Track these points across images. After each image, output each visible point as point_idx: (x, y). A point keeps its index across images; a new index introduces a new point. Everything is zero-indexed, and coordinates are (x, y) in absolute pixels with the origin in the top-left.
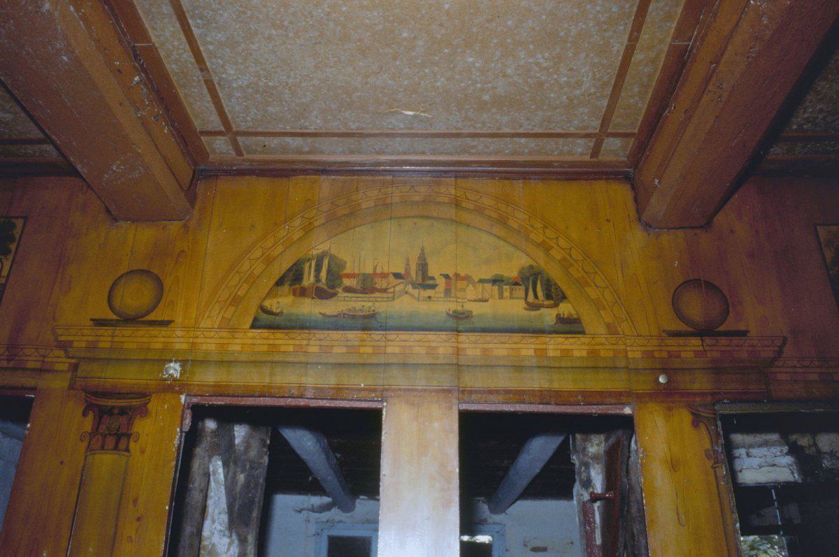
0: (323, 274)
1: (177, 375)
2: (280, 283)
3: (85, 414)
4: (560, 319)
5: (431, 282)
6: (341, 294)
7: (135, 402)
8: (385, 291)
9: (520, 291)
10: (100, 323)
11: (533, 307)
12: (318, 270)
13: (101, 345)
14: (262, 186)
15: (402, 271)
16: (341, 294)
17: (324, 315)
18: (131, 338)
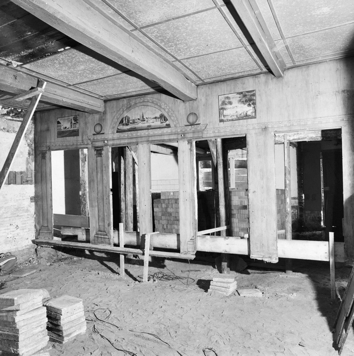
0: (127, 120)
1: (106, 143)
2: (120, 123)
3: (95, 151)
4: (166, 125)
5: (144, 120)
6: (130, 124)
7: (101, 148)
8: (137, 123)
9: (159, 119)
10: (94, 135)
11: (162, 123)
12: (126, 120)
13: (95, 139)
14: (114, 102)
15: (139, 118)
16: (130, 124)
18: (99, 137)
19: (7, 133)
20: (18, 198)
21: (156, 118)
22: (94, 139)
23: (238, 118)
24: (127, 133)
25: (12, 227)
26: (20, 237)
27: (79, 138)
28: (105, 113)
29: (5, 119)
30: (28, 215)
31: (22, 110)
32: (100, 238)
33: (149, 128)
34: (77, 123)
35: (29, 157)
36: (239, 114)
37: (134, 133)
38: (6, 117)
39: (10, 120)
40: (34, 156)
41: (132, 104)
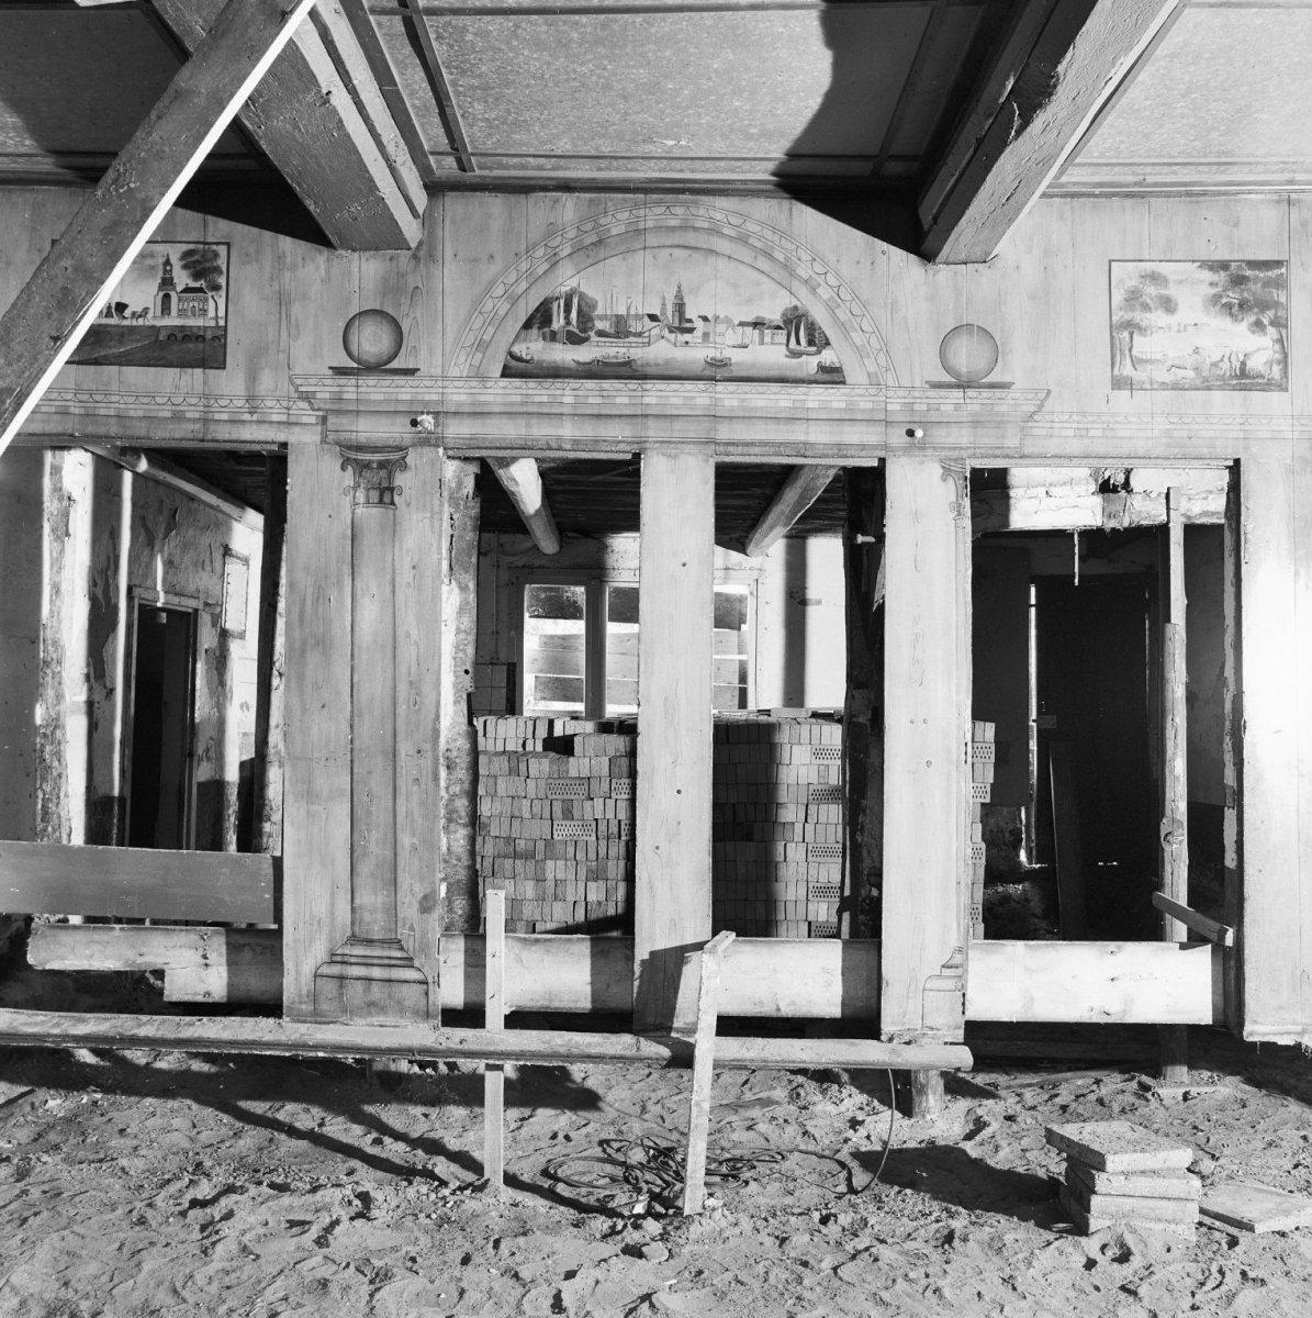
2: (527, 325)
4: (822, 368)
5: (688, 325)
7: (393, 456)
8: (640, 335)
10: (340, 371)
11: (795, 354)
12: (568, 310)
15: (658, 312)
17: (579, 363)
18: (375, 389)
21: (757, 324)
23: (1206, 380)
24: (575, 384)
27: (229, 383)
28: (425, 254)
32: (359, 986)
33: (716, 372)
36: (1208, 362)
37: (621, 394)
41: (614, 232)
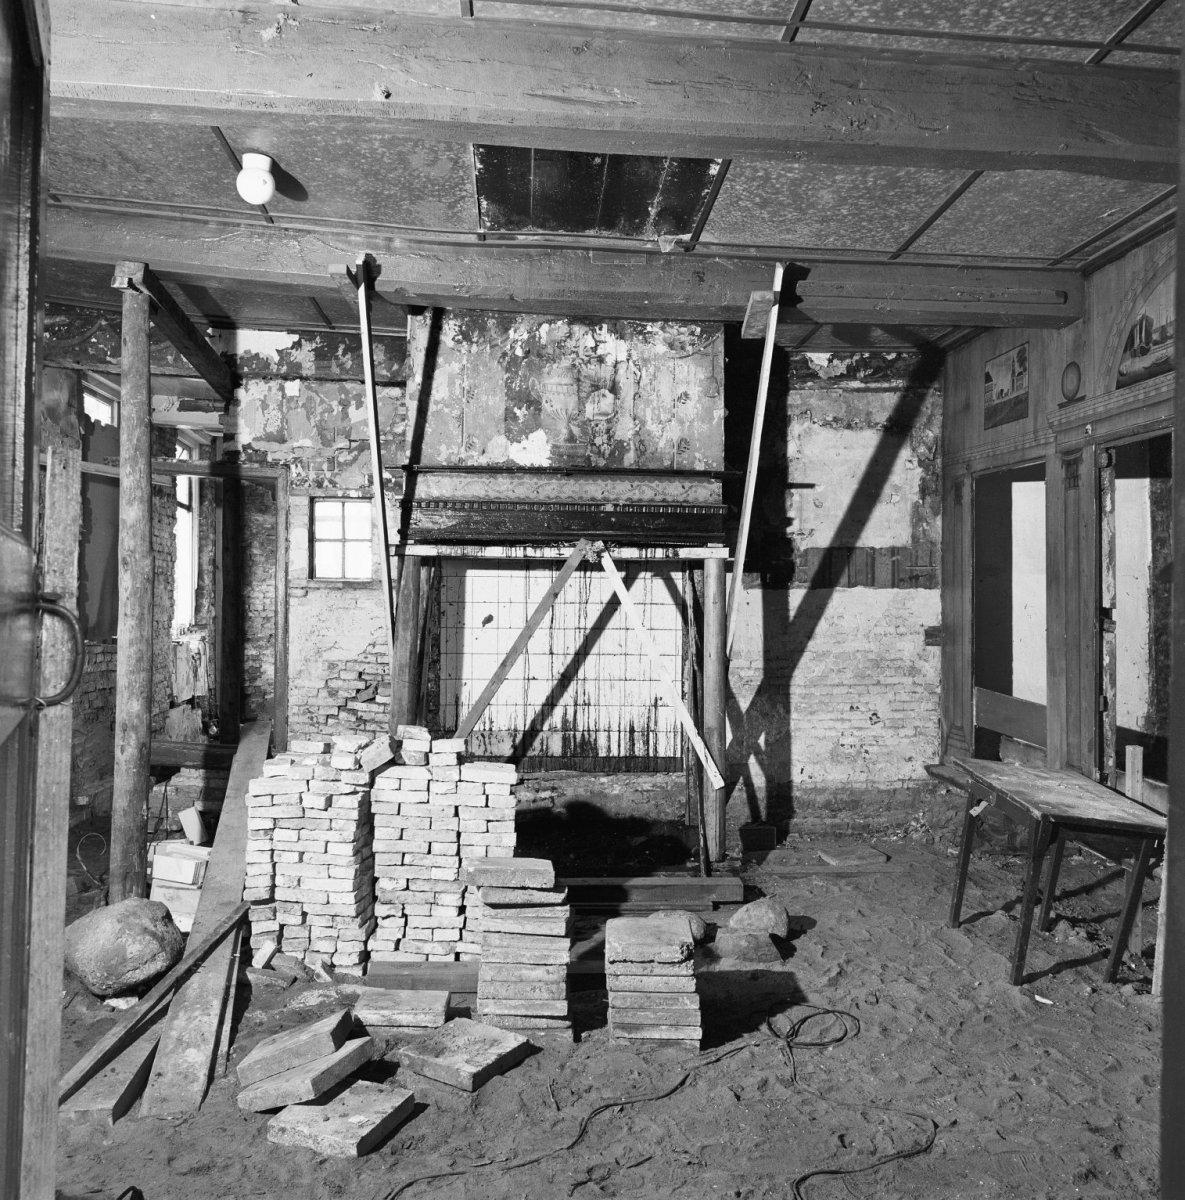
2: (1125, 351)
10: (1061, 406)
17: (1146, 368)
19: (847, 432)
20: (879, 630)
22: (1060, 424)
24: (1144, 384)
25: (855, 715)
26: (885, 750)
27: (1028, 423)
29: (841, 391)
30: (914, 683)
31: (899, 354)
34: (1025, 370)
35: (923, 498)
38: (843, 384)
39: (858, 390)
40: (938, 498)
